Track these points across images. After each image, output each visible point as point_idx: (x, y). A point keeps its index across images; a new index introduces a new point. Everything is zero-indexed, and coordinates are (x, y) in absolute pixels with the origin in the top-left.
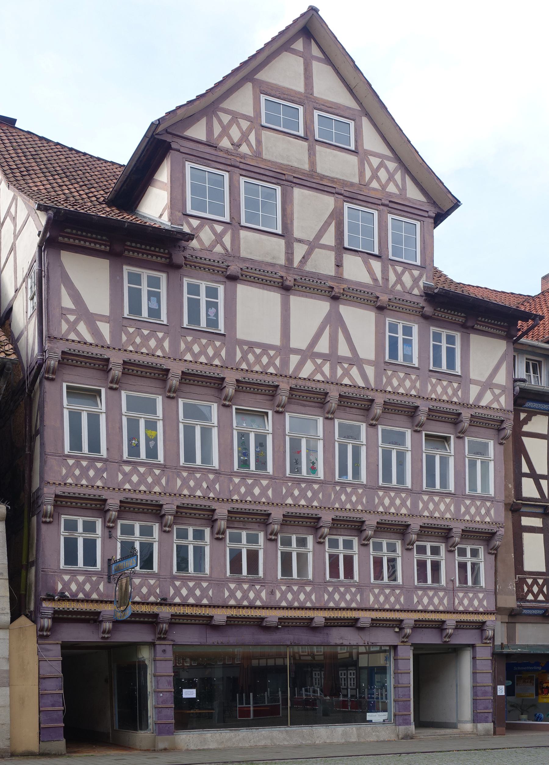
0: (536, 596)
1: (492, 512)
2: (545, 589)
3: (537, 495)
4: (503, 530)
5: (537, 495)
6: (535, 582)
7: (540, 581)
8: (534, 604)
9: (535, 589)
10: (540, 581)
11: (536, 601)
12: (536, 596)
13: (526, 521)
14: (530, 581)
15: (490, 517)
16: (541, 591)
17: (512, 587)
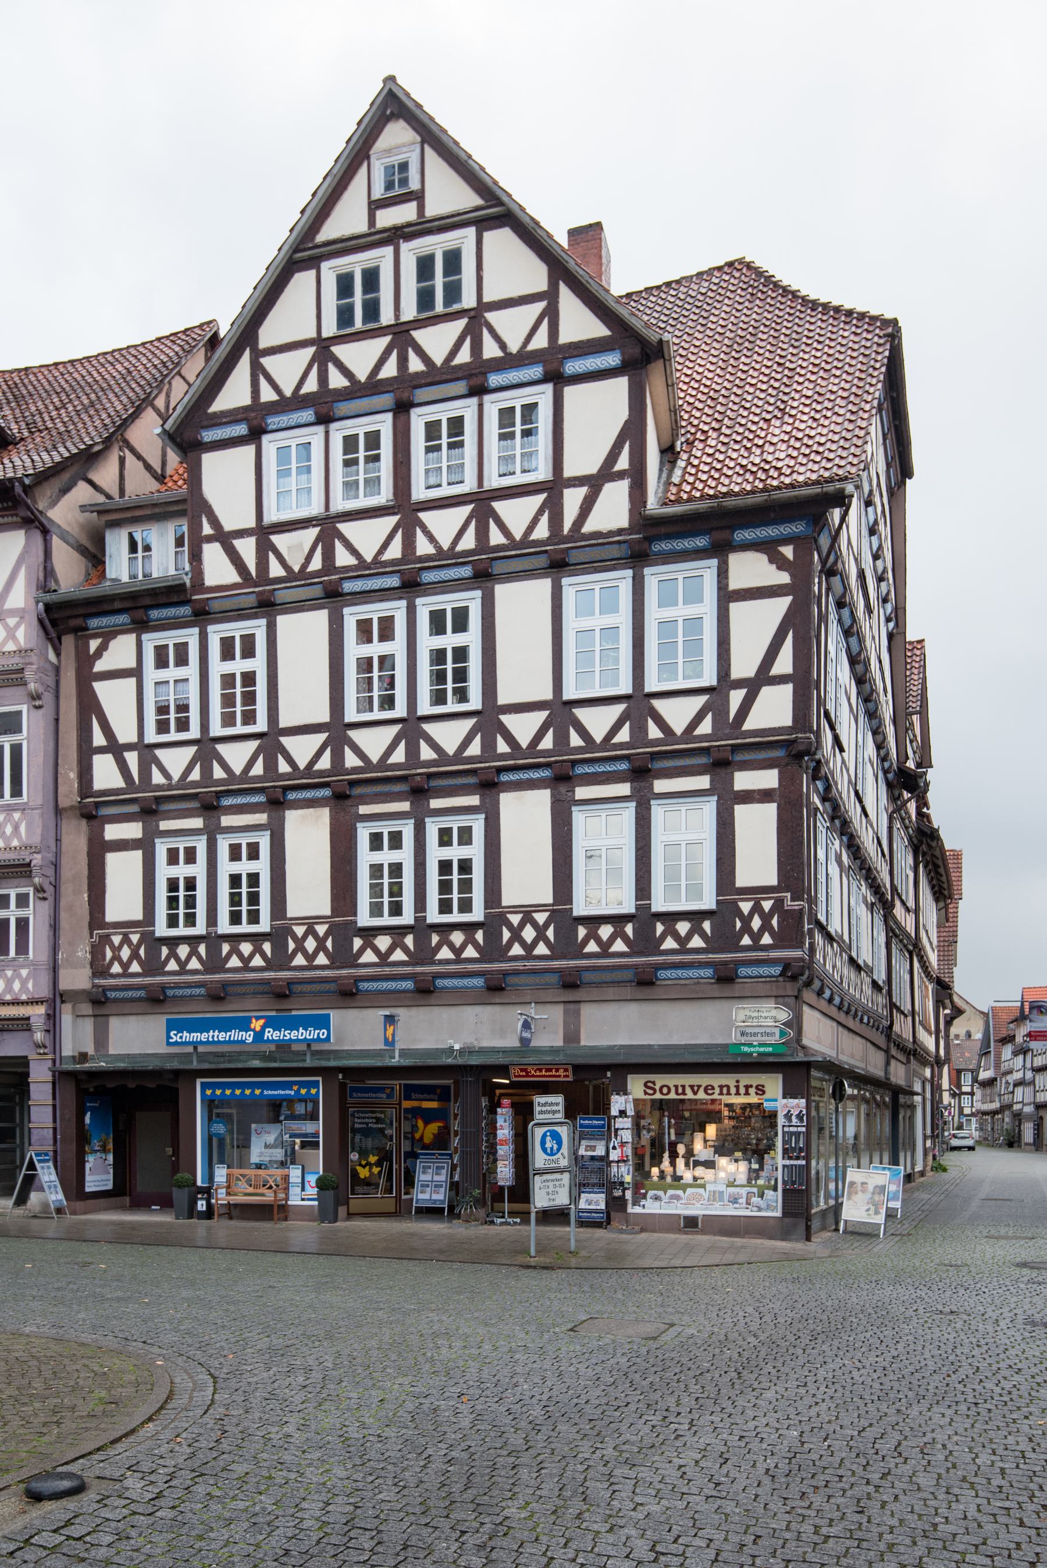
0: (125, 966)
1: (23, 829)
2: (142, 952)
3: (119, 783)
4: (39, 856)
5: (119, 783)
6: (126, 940)
7: (135, 938)
8: (123, 981)
9: (125, 953)
10: (135, 938)
11: (125, 974)
12: (125, 966)
13: (113, 832)
14: (116, 940)
15: (20, 838)
16: (134, 955)
17: (83, 952)
